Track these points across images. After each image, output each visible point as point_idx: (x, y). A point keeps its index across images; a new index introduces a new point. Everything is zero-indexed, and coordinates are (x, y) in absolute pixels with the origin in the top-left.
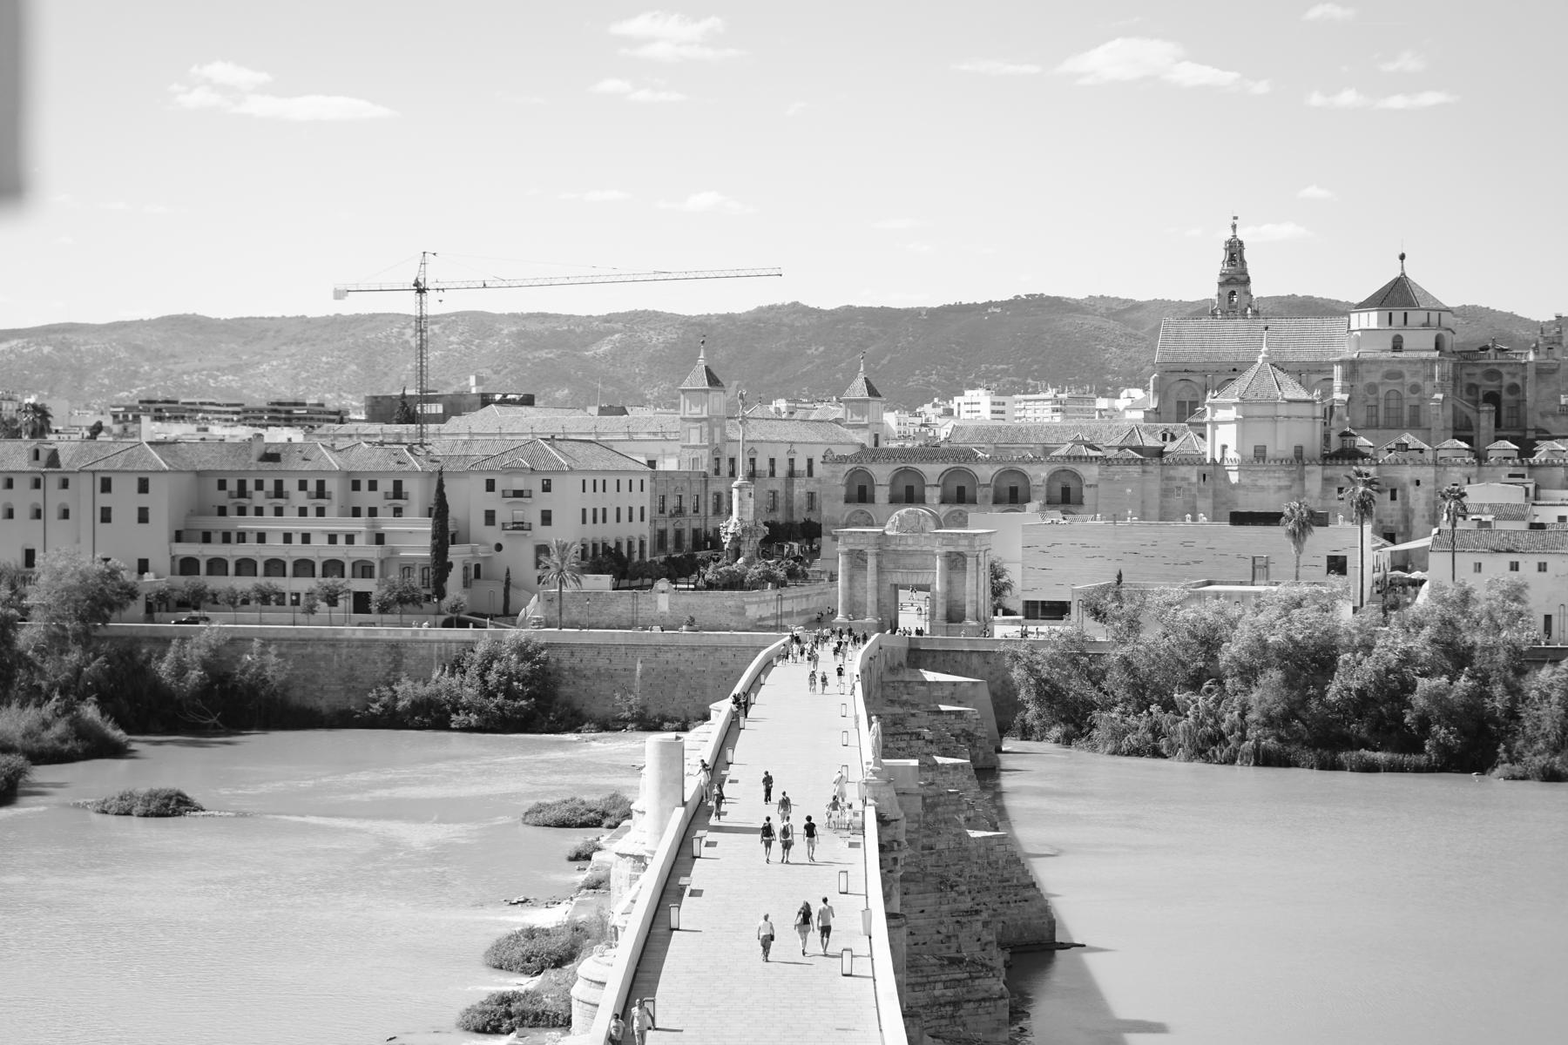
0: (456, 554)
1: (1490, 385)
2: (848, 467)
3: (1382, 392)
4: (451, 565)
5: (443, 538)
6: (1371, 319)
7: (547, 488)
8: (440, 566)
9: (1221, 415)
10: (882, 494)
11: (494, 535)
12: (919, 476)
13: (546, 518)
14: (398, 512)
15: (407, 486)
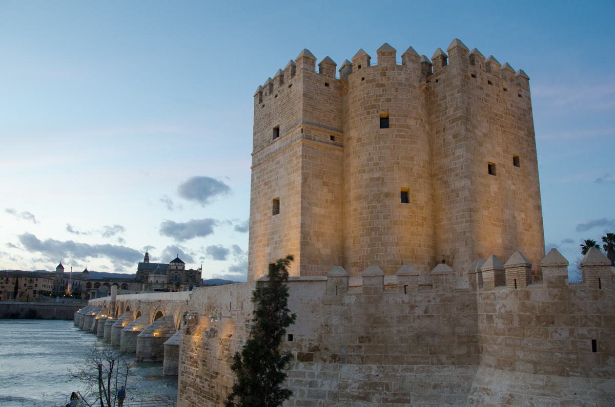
0: (19, 290)
1: (191, 275)
2: (87, 282)
3: (174, 275)
4: (17, 293)
5: (16, 288)
6: (173, 263)
7: (37, 280)
8: (16, 292)
9: (151, 275)
10: (93, 286)
11: (25, 288)
12: (100, 284)
13: (36, 285)
14: (7, 283)
15: (9, 279)
